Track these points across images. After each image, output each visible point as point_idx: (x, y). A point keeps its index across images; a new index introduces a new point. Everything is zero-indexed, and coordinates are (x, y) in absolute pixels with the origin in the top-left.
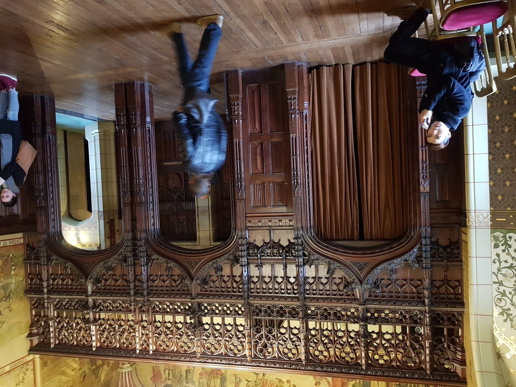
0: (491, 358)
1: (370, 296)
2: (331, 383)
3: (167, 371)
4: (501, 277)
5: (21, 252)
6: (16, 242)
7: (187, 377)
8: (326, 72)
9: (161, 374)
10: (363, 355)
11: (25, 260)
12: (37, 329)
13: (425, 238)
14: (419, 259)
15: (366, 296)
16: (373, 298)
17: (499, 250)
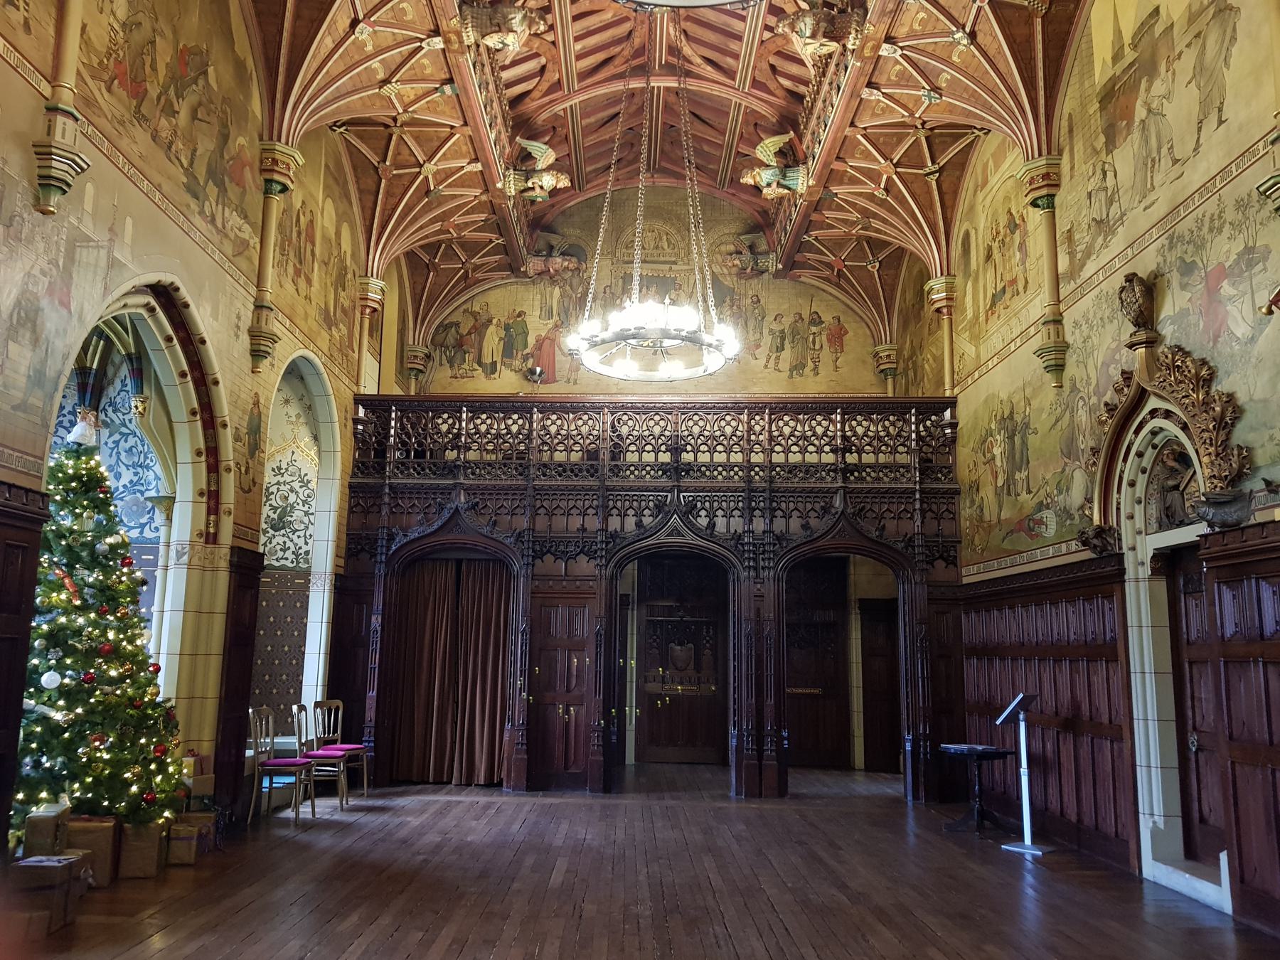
0: (323, 437)
1: (450, 494)
2: (557, 348)
3: (817, 347)
4: (306, 520)
5: (965, 554)
6: (974, 569)
7: (783, 339)
8: (481, 777)
9: (829, 340)
10: (464, 424)
11: (960, 542)
12: (945, 434)
13: (381, 562)
14: (391, 538)
15: (453, 495)
16: (447, 491)
17: (305, 548)
